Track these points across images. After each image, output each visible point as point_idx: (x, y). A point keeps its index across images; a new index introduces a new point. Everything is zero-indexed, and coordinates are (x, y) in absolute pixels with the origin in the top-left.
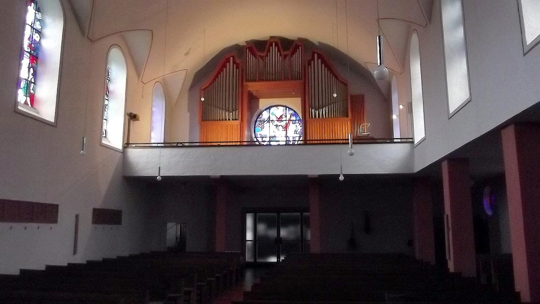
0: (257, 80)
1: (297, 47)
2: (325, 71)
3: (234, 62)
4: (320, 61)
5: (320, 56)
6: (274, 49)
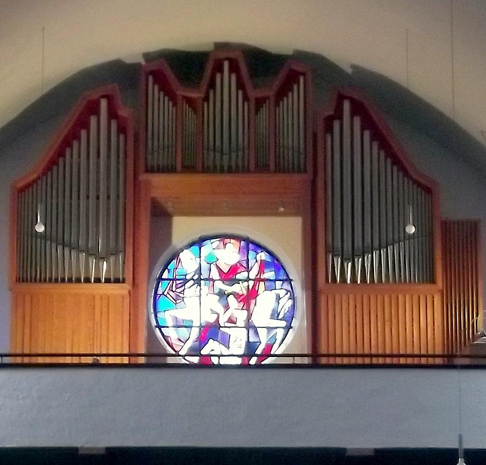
0: (179, 168)
1: (292, 78)
2: (372, 150)
3: (113, 114)
4: (357, 121)
5: (358, 108)
6: (227, 80)
